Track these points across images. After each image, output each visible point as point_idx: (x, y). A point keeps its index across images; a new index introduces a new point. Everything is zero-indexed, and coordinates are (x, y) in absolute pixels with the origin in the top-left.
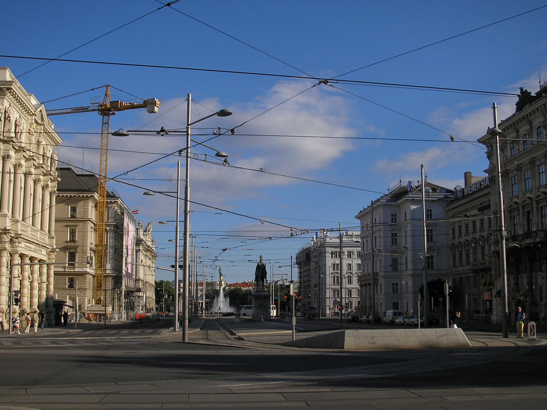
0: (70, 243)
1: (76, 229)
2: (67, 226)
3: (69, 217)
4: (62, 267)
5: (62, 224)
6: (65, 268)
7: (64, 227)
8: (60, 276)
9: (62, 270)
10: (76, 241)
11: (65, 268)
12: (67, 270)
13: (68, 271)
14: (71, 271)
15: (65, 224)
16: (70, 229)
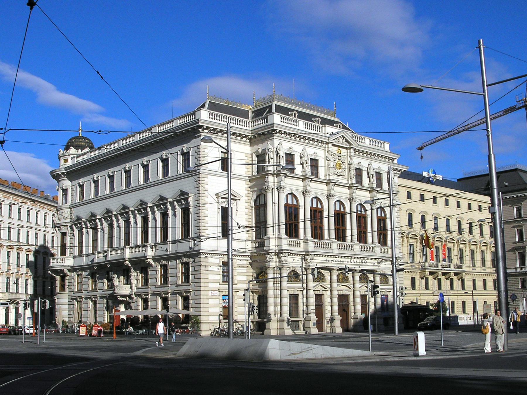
0: (519, 244)
1: (523, 229)
2: (514, 227)
3: (516, 217)
4: (514, 268)
5: (508, 225)
6: (516, 268)
7: (512, 229)
8: (513, 278)
9: (514, 271)
10: (524, 241)
11: (516, 268)
12: (518, 271)
13: (519, 271)
14: (522, 271)
15: (512, 225)
16: (517, 230)
